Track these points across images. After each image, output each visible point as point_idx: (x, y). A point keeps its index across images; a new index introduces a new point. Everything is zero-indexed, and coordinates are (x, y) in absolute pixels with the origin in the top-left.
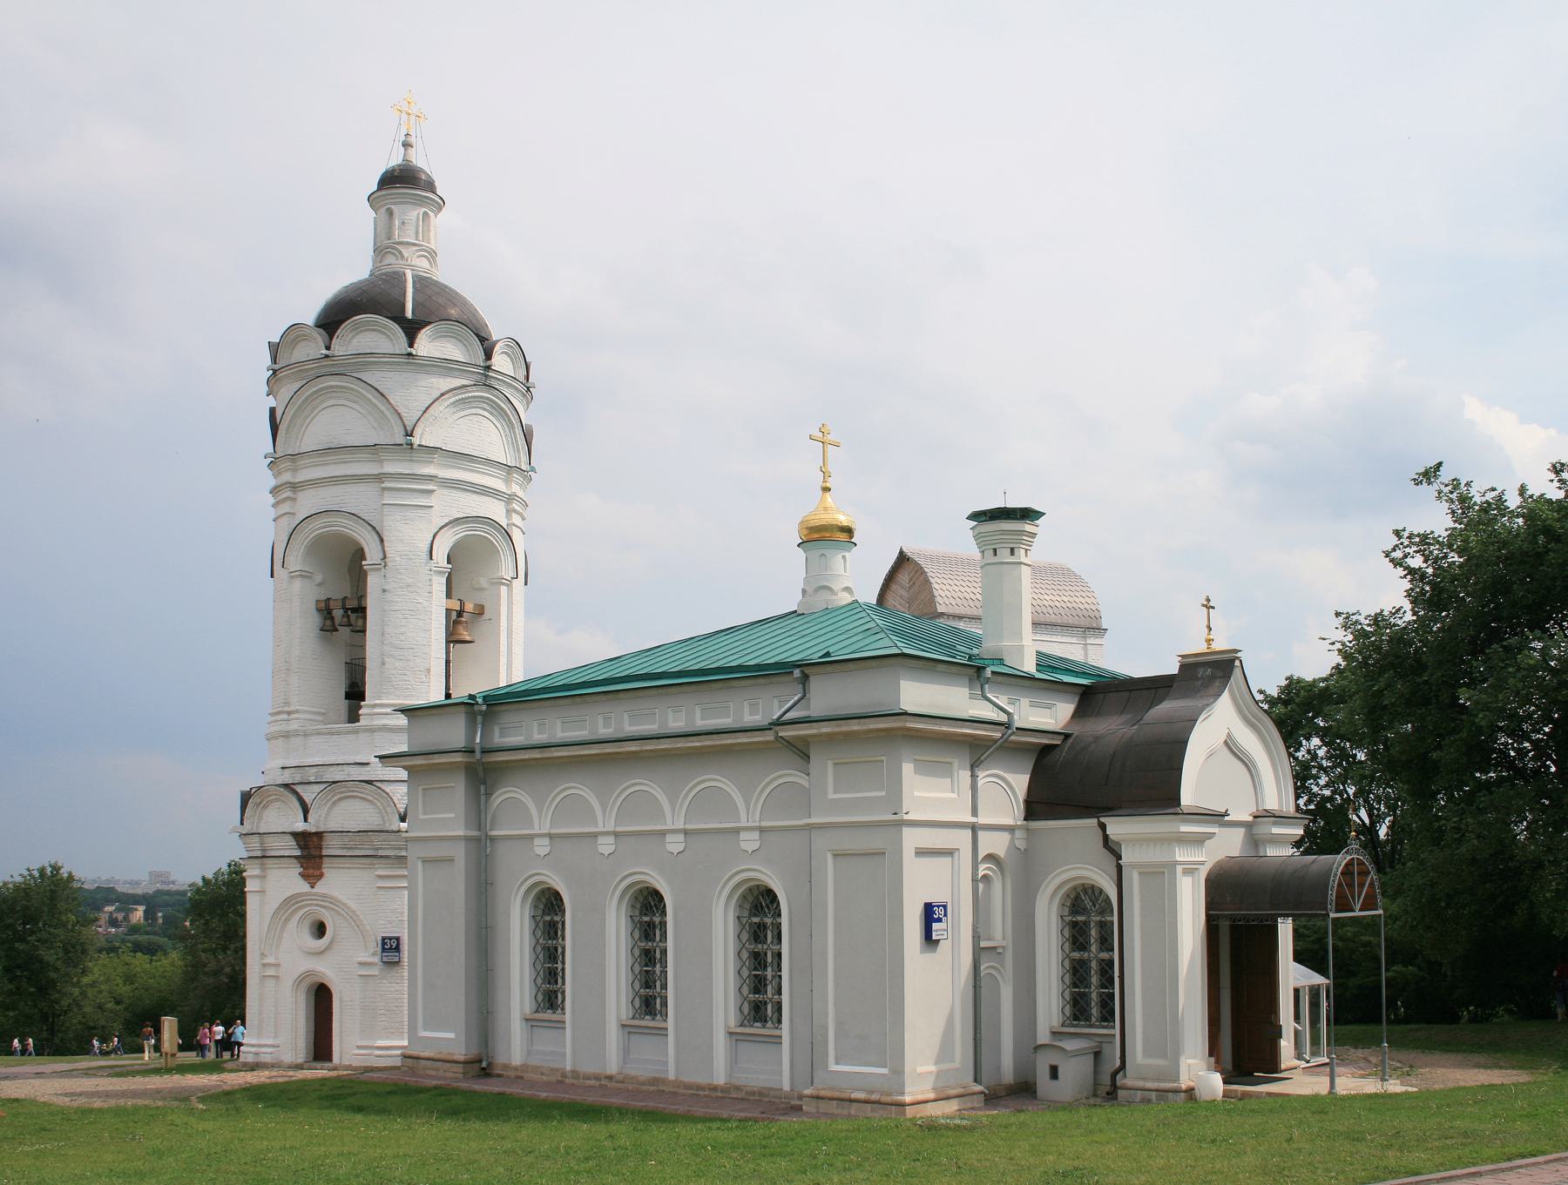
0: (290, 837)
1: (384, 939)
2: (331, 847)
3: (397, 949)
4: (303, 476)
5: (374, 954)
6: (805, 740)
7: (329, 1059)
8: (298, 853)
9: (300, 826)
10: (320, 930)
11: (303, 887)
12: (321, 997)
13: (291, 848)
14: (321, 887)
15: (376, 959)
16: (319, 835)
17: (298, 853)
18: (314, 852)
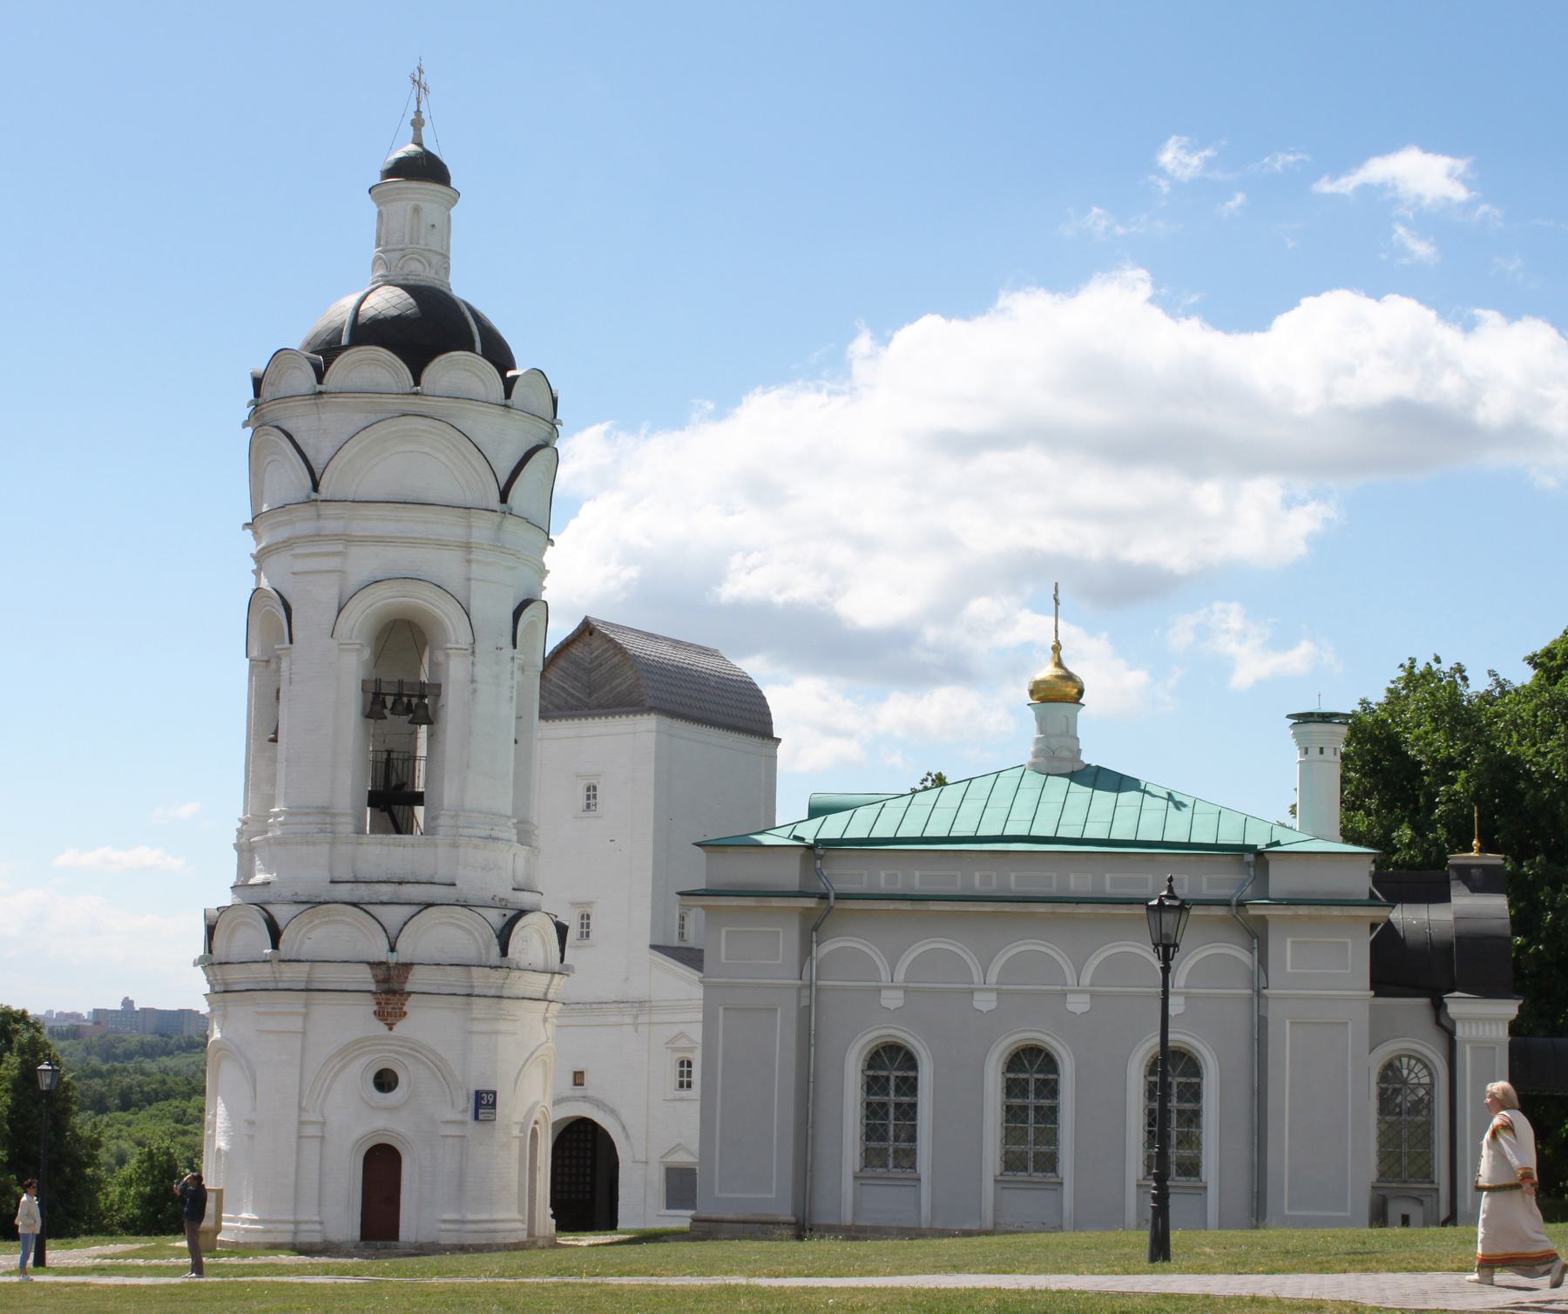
0: (367, 968)
1: (478, 1095)
2: (417, 980)
3: (493, 1105)
4: (358, 528)
5: (465, 1111)
6: (1263, 920)
7: (396, 1237)
8: (373, 987)
9: (380, 951)
10: (385, 1081)
11: (381, 1028)
12: (382, 1167)
13: (365, 977)
14: (400, 1027)
15: (469, 1115)
16: (408, 966)
17: (373, 987)
18: (396, 986)
